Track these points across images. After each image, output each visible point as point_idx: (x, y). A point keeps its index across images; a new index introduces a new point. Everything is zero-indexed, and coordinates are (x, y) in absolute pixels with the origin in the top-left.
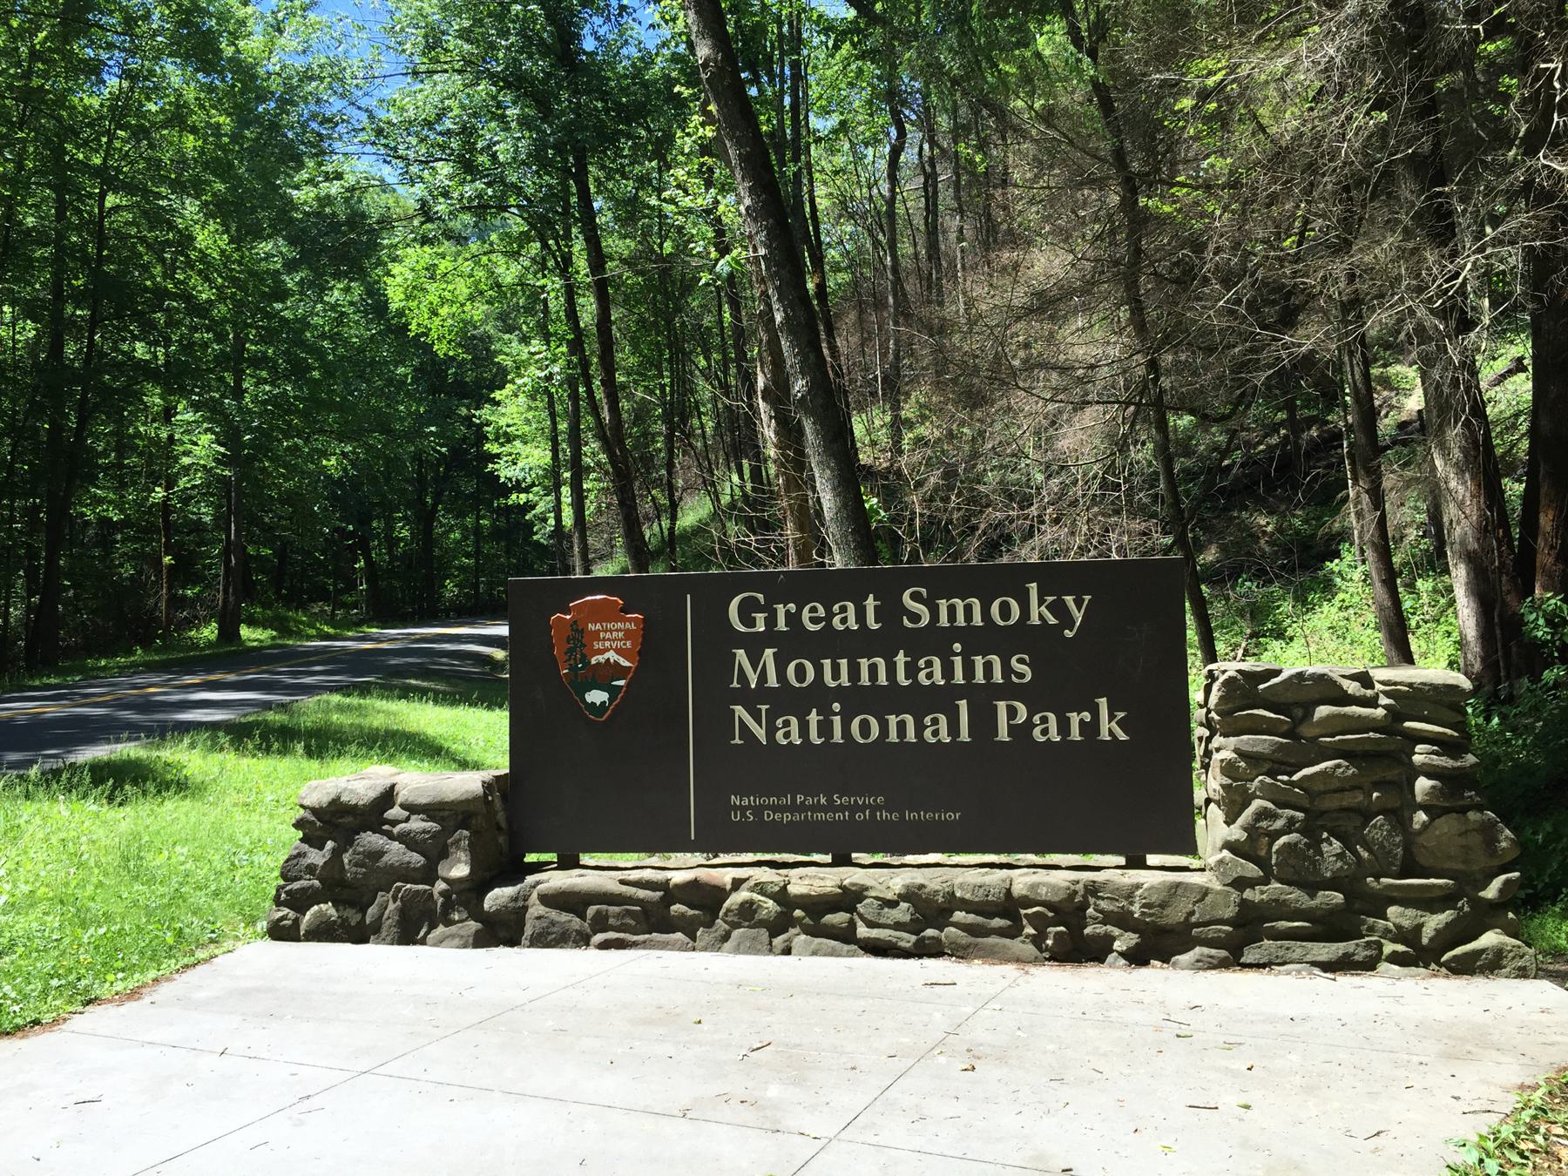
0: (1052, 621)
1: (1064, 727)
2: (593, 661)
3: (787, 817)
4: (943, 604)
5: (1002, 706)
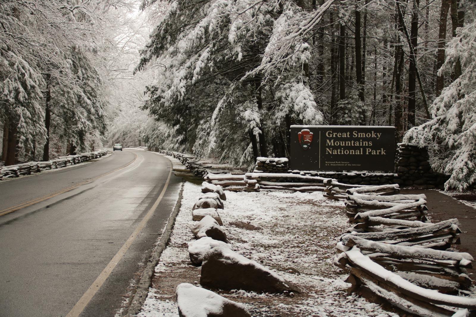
1: (376, 152)
3: (334, 165)
4: (359, 134)
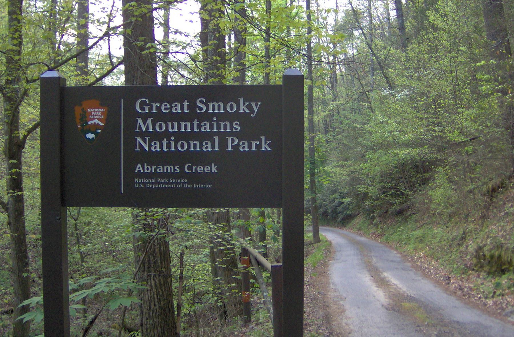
2: (89, 123)
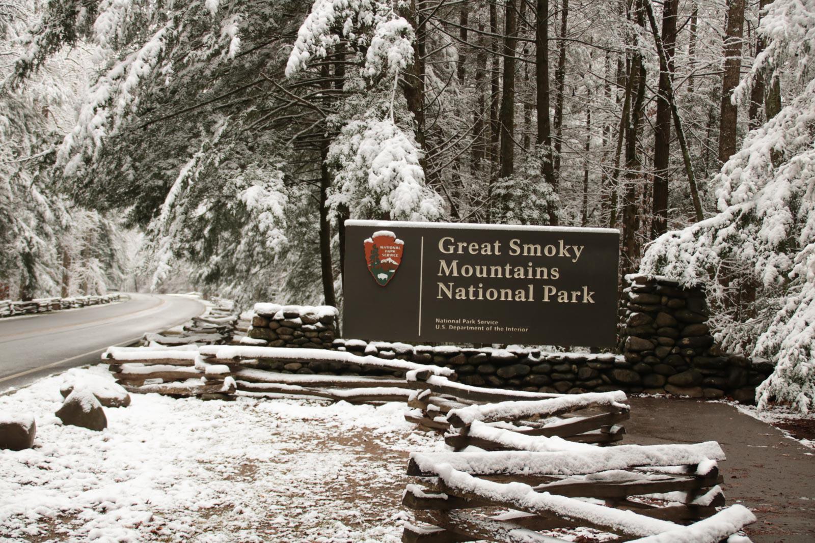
0: (568, 255)
1: (570, 297)
3: (458, 328)
4: (526, 247)
5: (546, 288)
